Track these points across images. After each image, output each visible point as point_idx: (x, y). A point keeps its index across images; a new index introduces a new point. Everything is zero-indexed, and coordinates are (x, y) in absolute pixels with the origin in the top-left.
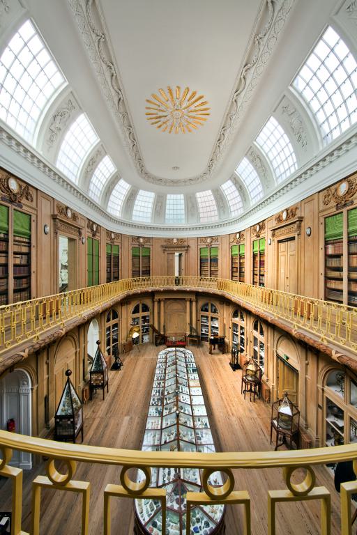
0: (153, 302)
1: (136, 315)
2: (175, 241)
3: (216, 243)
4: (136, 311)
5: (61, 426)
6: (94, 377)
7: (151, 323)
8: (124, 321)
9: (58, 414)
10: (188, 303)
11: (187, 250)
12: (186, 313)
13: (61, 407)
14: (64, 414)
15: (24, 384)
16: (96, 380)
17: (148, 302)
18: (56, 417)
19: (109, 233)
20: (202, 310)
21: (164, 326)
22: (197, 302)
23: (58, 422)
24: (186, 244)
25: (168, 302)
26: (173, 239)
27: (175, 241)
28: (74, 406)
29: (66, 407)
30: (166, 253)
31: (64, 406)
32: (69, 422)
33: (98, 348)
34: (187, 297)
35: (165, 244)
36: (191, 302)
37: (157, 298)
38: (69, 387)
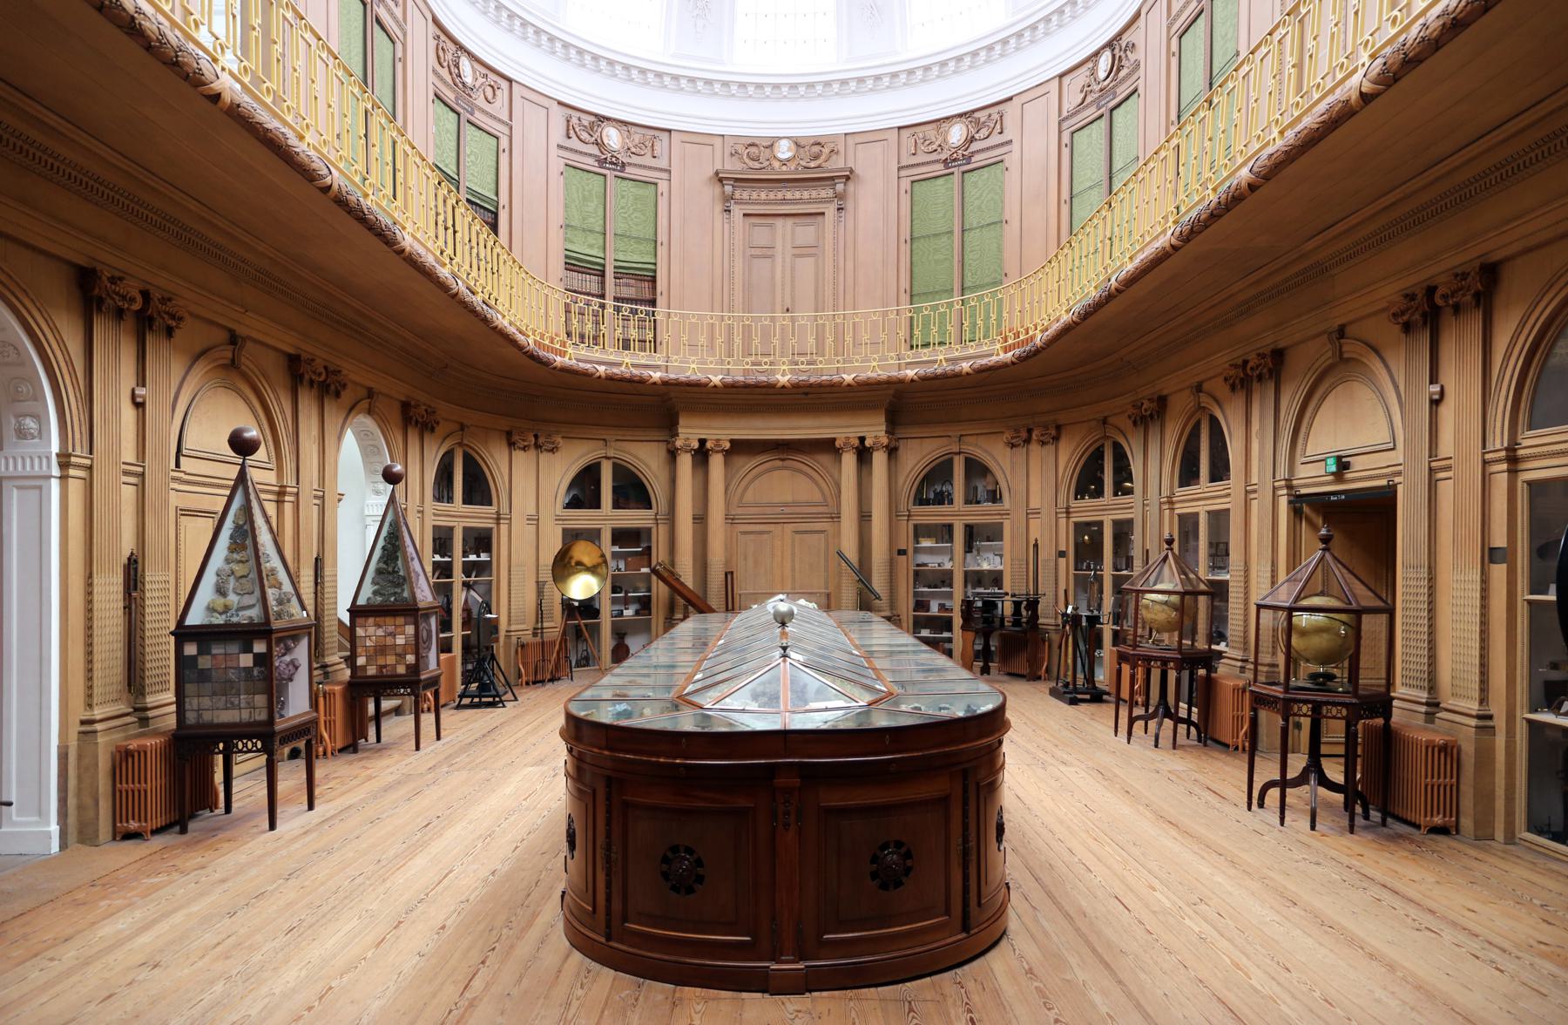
0: (673, 454)
1: (583, 518)
2: (784, 151)
3: (996, 139)
4: (584, 491)
5: (204, 676)
6: (370, 633)
7: (660, 554)
8: (523, 502)
9: (195, 618)
10: (849, 461)
11: (840, 197)
12: (835, 517)
13: (206, 593)
14: (219, 620)
15: (22, 434)
16: (381, 650)
17: (646, 458)
18: (183, 633)
19: (448, 45)
20: (921, 501)
21: (729, 575)
22: (892, 452)
23: (194, 659)
24: (838, 163)
25: (746, 464)
26: (771, 144)
27: (784, 151)
28: (271, 593)
29: (233, 598)
30: (737, 211)
31: (220, 591)
32: (246, 660)
33: (392, 500)
34: (843, 429)
35: (733, 166)
36: (863, 454)
37: (690, 432)
38: (247, 509)
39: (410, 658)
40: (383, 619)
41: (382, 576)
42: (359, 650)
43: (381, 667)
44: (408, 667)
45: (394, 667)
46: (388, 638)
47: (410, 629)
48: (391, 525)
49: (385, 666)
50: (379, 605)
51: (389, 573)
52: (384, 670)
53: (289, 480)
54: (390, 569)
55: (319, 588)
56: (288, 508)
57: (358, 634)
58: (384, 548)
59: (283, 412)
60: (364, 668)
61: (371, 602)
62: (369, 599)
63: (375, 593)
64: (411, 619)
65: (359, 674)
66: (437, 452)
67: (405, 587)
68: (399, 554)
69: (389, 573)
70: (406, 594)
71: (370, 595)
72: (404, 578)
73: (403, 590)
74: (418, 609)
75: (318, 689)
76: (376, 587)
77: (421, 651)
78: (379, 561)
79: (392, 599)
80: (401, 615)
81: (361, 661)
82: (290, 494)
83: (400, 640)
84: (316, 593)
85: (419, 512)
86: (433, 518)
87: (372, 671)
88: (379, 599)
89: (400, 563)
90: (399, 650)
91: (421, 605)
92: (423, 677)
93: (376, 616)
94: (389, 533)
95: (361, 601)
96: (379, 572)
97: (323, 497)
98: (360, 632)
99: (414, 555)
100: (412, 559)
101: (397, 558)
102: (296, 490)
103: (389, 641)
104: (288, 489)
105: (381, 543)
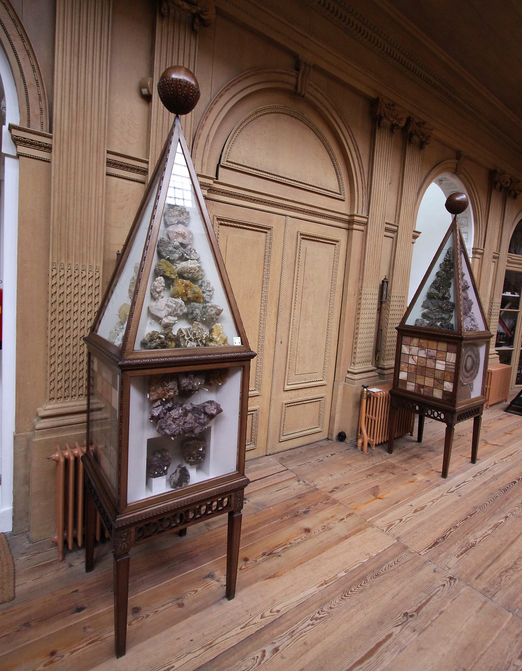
39: (448, 386)
40: (427, 341)
41: (433, 301)
42: (402, 365)
43: (419, 386)
44: (445, 393)
45: (432, 390)
46: (429, 361)
47: (452, 357)
48: (448, 253)
49: (423, 386)
50: (425, 329)
51: (439, 298)
52: (422, 390)
53: (360, 210)
54: (440, 295)
55: (384, 305)
56: (357, 236)
57: (402, 352)
58: (438, 274)
59: (357, 150)
60: (404, 382)
61: (418, 324)
62: (417, 320)
63: (424, 316)
64: (454, 348)
65: (400, 386)
66: (516, 218)
67: (453, 313)
68: (452, 281)
69: (439, 298)
70: (453, 321)
71: (419, 317)
72: (453, 305)
73: (451, 317)
74: (462, 339)
75: (362, 392)
76: (426, 311)
77: (461, 378)
78: (431, 287)
79: (439, 324)
80: (444, 342)
81: (403, 375)
82: (360, 223)
83: (440, 366)
84: (380, 310)
85: (494, 257)
86: (507, 263)
87: (411, 387)
88: (427, 322)
89: (451, 290)
90: (438, 375)
91: (466, 334)
92: (459, 408)
93: (420, 338)
94: (445, 260)
95: (410, 322)
96: (430, 296)
97: (397, 231)
98: (405, 349)
99: (470, 284)
100: (466, 288)
101: (449, 285)
102: (365, 220)
103: (430, 363)
104: (356, 218)
105: (436, 269)
